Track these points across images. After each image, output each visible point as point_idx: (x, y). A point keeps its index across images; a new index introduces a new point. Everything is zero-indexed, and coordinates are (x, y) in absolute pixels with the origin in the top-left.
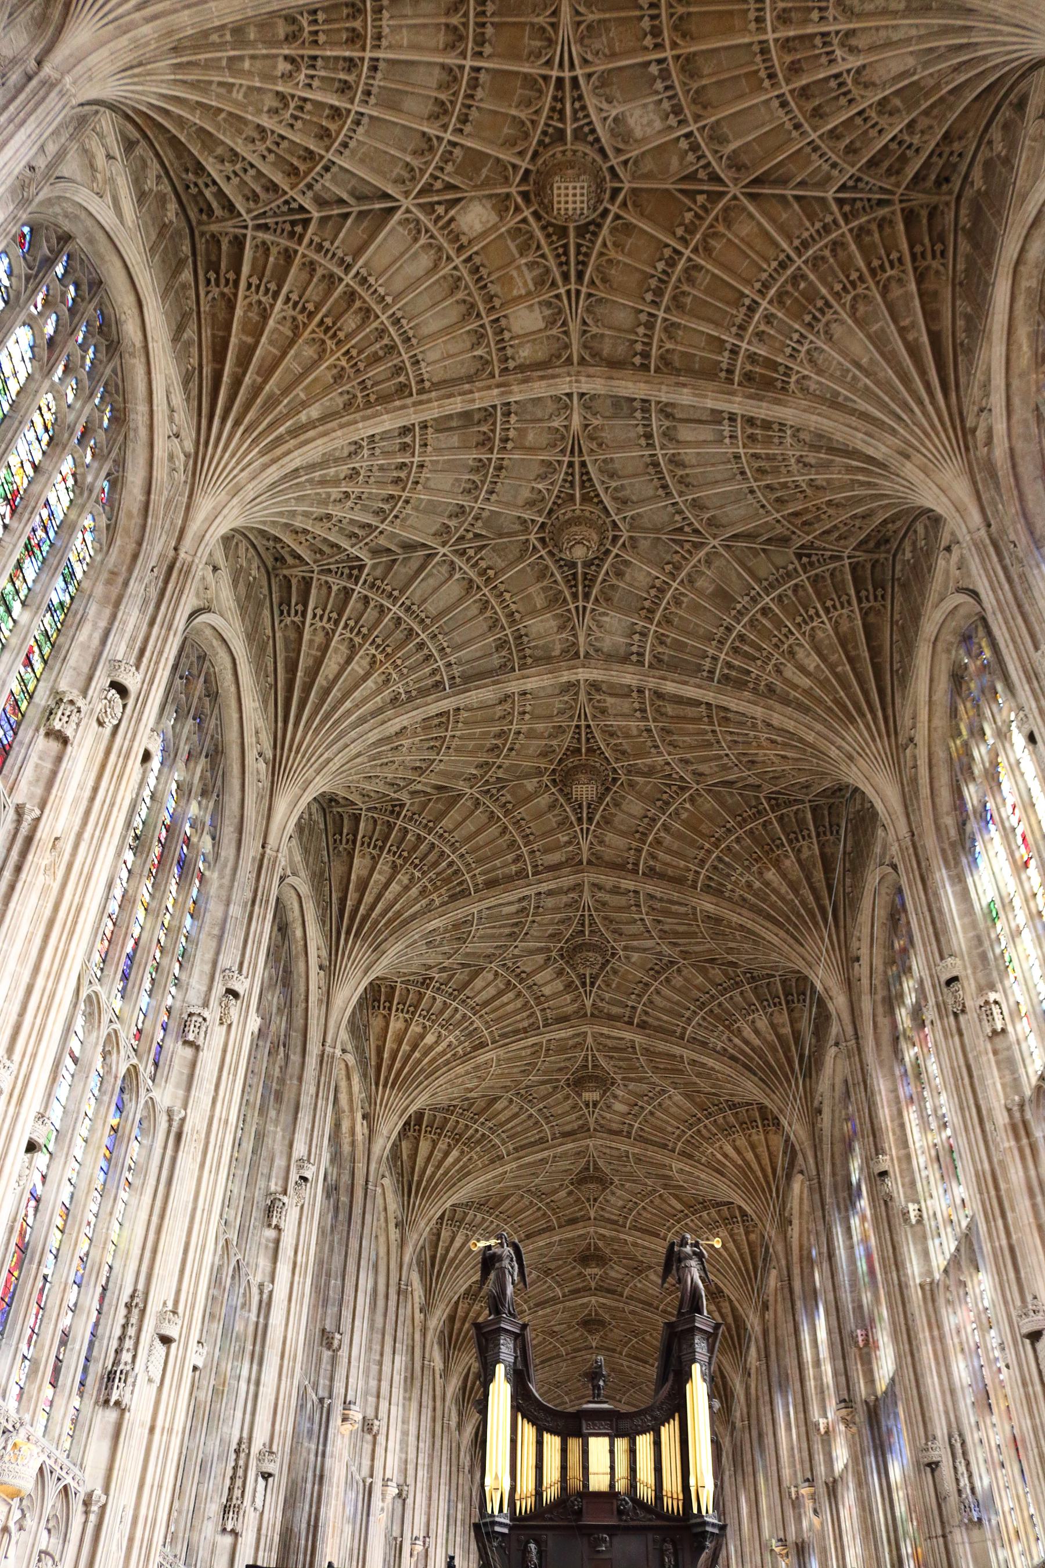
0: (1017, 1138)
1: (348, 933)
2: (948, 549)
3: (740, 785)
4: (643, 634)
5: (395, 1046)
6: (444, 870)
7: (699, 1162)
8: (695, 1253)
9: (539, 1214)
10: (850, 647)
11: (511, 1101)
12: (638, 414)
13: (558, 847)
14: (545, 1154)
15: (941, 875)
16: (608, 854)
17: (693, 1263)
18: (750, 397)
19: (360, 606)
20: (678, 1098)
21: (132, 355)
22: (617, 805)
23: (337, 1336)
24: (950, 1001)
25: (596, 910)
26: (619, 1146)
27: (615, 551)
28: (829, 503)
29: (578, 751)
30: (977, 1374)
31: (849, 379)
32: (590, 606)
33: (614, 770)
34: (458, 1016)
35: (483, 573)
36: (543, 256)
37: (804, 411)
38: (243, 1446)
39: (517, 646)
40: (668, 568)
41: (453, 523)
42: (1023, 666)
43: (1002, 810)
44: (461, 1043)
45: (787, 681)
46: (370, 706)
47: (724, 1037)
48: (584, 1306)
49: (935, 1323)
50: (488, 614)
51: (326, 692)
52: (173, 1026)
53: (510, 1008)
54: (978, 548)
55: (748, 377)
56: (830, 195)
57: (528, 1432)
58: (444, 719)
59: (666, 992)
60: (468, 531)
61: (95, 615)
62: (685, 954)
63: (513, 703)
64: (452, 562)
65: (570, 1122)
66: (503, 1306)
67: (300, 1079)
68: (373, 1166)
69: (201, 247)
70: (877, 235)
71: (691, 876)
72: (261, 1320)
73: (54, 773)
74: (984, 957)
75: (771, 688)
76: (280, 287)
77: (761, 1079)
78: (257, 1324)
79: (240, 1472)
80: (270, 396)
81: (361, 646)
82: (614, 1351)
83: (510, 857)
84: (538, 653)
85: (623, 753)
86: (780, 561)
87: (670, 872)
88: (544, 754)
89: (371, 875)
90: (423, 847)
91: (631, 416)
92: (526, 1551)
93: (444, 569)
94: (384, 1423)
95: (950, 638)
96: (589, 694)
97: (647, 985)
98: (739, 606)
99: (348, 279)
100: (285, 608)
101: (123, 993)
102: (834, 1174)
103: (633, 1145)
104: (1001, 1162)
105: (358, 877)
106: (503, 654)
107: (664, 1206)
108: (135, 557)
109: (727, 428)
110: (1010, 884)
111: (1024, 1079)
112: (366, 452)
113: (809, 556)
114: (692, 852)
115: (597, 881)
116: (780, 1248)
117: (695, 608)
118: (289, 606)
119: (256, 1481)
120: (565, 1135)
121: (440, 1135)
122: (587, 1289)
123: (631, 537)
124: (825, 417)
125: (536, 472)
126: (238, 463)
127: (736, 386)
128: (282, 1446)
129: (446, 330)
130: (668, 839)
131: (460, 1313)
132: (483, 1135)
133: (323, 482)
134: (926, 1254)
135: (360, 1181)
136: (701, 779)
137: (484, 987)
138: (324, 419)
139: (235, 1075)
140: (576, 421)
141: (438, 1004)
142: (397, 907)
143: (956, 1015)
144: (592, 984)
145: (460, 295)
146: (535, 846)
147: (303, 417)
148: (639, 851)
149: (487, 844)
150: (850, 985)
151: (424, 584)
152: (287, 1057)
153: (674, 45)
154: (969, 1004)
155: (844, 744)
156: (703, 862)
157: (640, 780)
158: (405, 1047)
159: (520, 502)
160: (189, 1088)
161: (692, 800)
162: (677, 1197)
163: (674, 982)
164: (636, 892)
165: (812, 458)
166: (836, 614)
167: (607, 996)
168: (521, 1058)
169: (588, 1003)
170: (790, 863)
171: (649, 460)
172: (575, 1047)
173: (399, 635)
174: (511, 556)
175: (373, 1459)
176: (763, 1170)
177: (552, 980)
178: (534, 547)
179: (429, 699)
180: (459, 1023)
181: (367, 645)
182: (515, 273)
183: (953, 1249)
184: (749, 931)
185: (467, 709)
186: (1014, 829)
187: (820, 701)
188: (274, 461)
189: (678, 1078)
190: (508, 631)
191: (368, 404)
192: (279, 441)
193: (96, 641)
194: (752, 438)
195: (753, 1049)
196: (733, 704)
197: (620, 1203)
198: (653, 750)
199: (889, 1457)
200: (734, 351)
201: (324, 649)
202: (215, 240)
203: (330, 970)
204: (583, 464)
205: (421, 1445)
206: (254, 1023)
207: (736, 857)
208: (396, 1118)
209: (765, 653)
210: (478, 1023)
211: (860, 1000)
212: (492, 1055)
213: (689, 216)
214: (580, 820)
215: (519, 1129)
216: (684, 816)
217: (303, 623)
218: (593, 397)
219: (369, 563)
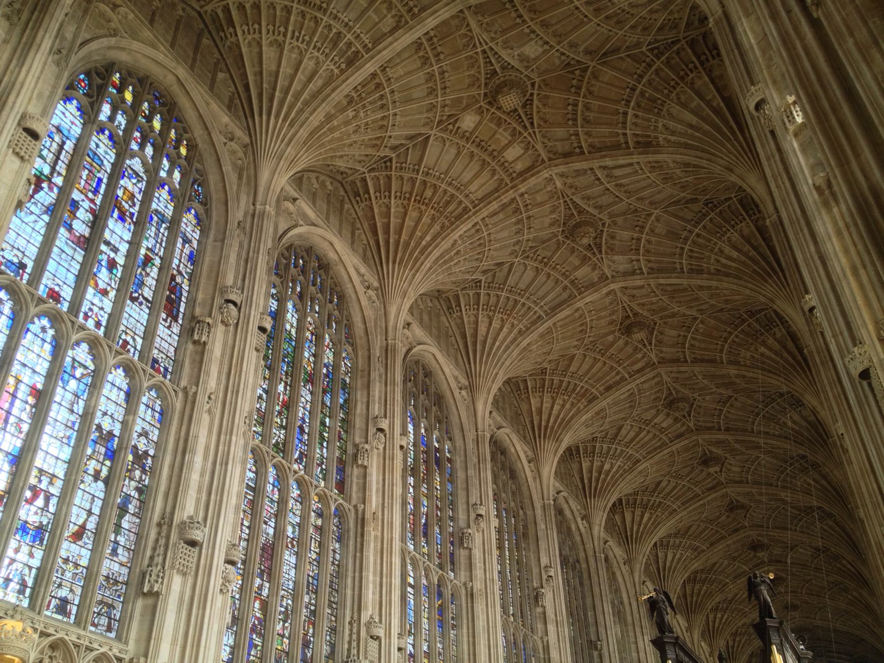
4: (638, 260)
10: (753, 241)
13: (639, 360)
14: (701, 502)
19: (487, 297)
21: (336, 265)
32: (604, 256)
33: (653, 320)
34: (618, 451)
36: (509, 123)
37: (672, 153)
40: (637, 229)
41: (517, 248)
45: (724, 266)
46: (509, 339)
50: (552, 278)
51: (484, 343)
52: (457, 542)
56: (644, 49)
61: (360, 396)
68: (596, 543)
69: (348, 188)
70: (677, 59)
73: (365, 483)
75: (718, 270)
76: (390, 192)
80: (405, 241)
81: (494, 316)
85: (654, 310)
87: (706, 358)
88: (611, 323)
90: (564, 385)
93: (521, 267)
99: (419, 177)
101: (427, 543)
108: (369, 357)
129: (476, 176)
130: (697, 344)
133: (445, 262)
135: (590, 553)
137: (628, 433)
138: (434, 239)
140: (559, 184)
142: (561, 416)
145: (476, 158)
147: (424, 243)
152: (525, 513)
153: (532, 19)
156: (721, 351)
158: (595, 474)
160: (471, 571)
161: (702, 322)
169: (691, 425)
170: (771, 341)
172: (694, 446)
173: (511, 303)
179: (537, 325)
180: (620, 455)
182: (499, 136)
188: (417, 271)
191: (452, 223)
192: (417, 260)
193: (365, 410)
194: (654, 167)
200: (625, 134)
201: (477, 323)
202: (353, 182)
203: (534, 460)
206: (495, 522)
213: (574, 82)
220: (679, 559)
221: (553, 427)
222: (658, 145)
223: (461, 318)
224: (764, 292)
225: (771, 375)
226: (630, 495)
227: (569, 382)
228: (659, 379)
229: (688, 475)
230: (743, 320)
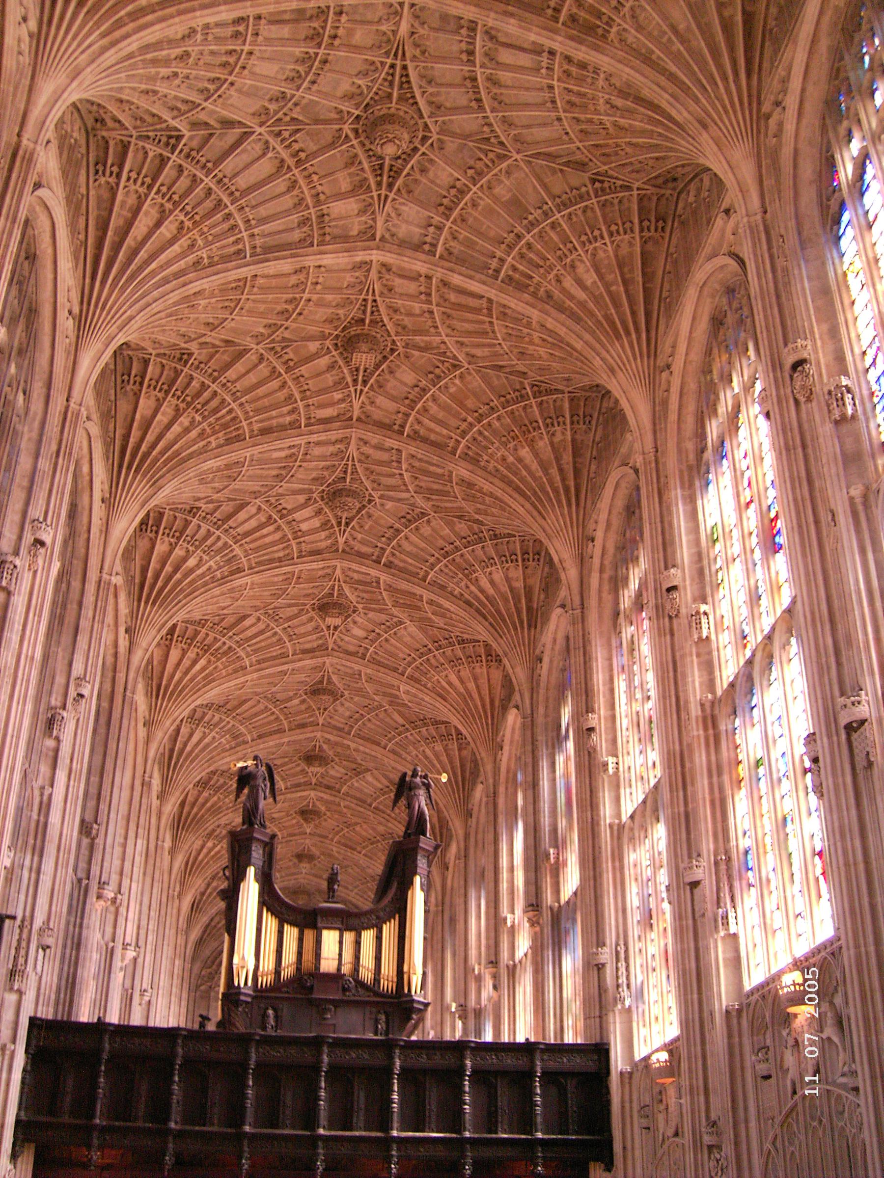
0: (706, 729)
1: (129, 468)
2: (727, 212)
3: (508, 370)
4: (440, 228)
5: (158, 567)
6: (223, 416)
7: (425, 686)
8: (424, 784)
9: (272, 718)
10: (626, 270)
11: (259, 619)
12: (464, 32)
13: (332, 404)
14: (285, 667)
15: (677, 494)
16: (377, 415)
17: (422, 793)
18: (572, 38)
19: (174, 173)
20: (413, 629)
22: (391, 372)
23: (95, 826)
24: (668, 607)
25: (360, 461)
26: (353, 665)
27: (423, 149)
28: (630, 144)
29: (363, 321)
30: (645, 899)
31: (665, 40)
32: (392, 196)
34: (220, 544)
35: (295, 154)
37: (620, 61)
38: (26, 923)
39: (319, 223)
40: (470, 172)
41: (272, 107)
42: (772, 355)
43: (736, 452)
44: (220, 568)
45: (564, 291)
46: (174, 268)
47: (463, 584)
48: (304, 798)
49: (618, 856)
50: (295, 192)
51: (135, 252)
53: (267, 540)
54: (752, 232)
55: (573, 18)
57: (270, 923)
58: (241, 284)
59: (413, 538)
60: (285, 114)
62: (437, 509)
63: (308, 273)
64: (267, 142)
65: (311, 641)
66: (255, 818)
67: (80, 604)
68: (132, 675)
71: (452, 444)
72: (42, 818)
74: (701, 572)
75: (549, 296)
77: (491, 624)
78: (38, 821)
79: (24, 944)
81: (171, 212)
82: (326, 837)
83: (285, 410)
84: (337, 232)
85: (404, 328)
86: (575, 182)
87: (433, 437)
89: (154, 415)
90: (206, 395)
91: (456, 32)
92: (265, 1016)
93: (258, 148)
94: (126, 897)
95: (717, 287)
96: (380, 272)
97: (398, 531)
98: (530, 217)
100: (100, 168)
102: (546, 716)
104: (689, 746)
105: (142, 417)
106: (304, 229)
107: (388, 720)
109: (546, 61)
110: (731, 518)
111: (718, 681)
112: (199, 37)
113: (602, 182)
114: (454, 422)
115: (364, 437)
116: (489, 767)
117: (490, 212)
118: (105, 166)
119: (37, 951)
120: (305, 652)
121: (190, 645)
122: (308, 784)
123: (439, 139)
124: (637, 71)
125: (359, 68)
126: (79, 46)
127: (560, 25)
128: (59, 924)
130: (434, 409)
131: (190, 798)
132: (230, 648)
133: (155, 62)
134: (617, 800)
135: (120, 689)
136: (473, 360)
139: (40, 616)
141: (203, 532)
143: (670, 617)
144: (347, 524)
146: (310, 401)
148: (407, 415)
149: (266, 396)
150: (582, 560)
151: (237, 159)
152: (69, 584)
154: (683, 611)
155: (608, 357)
156: (464, 433)
157: (416, 353)
158: (168, 568)
159: (339, 93)
161: (461, 377)
162: (400, 713)
163: (422, 531)
164: (399, 451)
165: (619, 102)
166: (619, 238)
167: (359, 536)
168: (274, 584)
169: (341, 540)
170: (543, 444)
171: (467, 75)
173: (209, 204)
174: (323, 142)
175: (115, 927)
176: (482, 699)
177: (312, 517)
178: (347, 136)
181: (177, 212)
183: (640, 801)
184: (496, 498)
185: (263, 277)
186: (742, 474)
187: (592, 314)
188: (113, 44)
189: (417, 614)
190: (312, 211)
192: (119, 24)
194: (567, 73)
195: (487, 598)
196: (512, 303)
197: (347, 714)
198: (432, 330)
199: (564, 952)
201: (136, 211)
203: (109, 503)
204: (405, 67)
207: (495, 432)
208: (154, 632)
209: (548, 263)
210: (238, 551)
211: (589, 576)
212: (248, 580)
214: (355, 381)
215: (263, 644)
216: (452, 390)
217: (118, 185)
218: (422, 9)
219: (187, 134)
220: (208, 745)
221: (156, 460)
222: (604, 37)
223: (113, 191)
224: (604, 354)
225: (516, 496)
226: (193, 623)
227: (215, 394)
228: (342, 447)
229: (290, 619)
230: (522, 396)
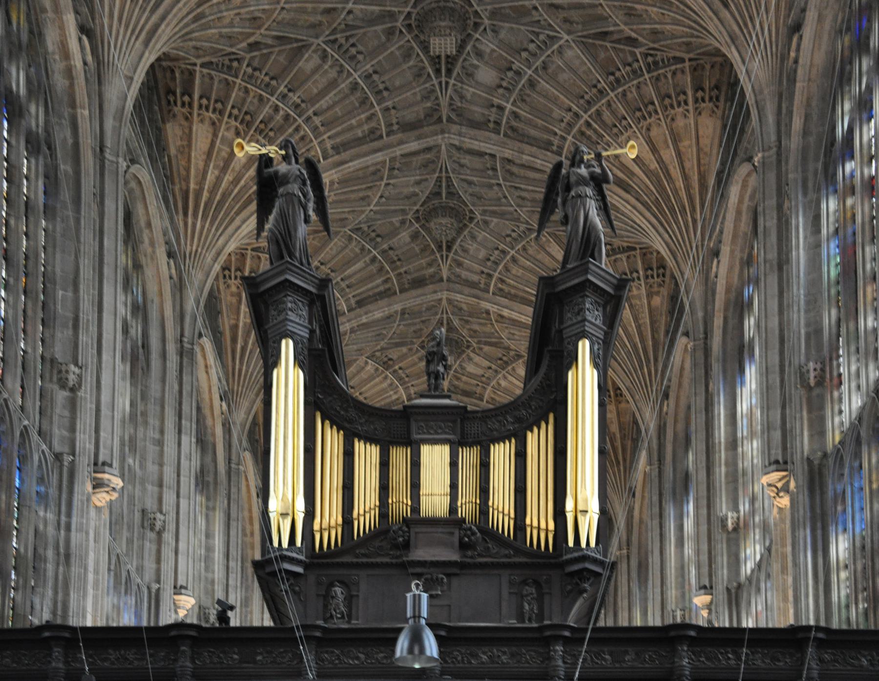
14: (379, 157)
103: (503, 145)
132: (287, 117)
197: (482, 254)
205: (232, 564)
